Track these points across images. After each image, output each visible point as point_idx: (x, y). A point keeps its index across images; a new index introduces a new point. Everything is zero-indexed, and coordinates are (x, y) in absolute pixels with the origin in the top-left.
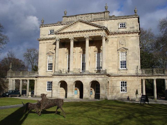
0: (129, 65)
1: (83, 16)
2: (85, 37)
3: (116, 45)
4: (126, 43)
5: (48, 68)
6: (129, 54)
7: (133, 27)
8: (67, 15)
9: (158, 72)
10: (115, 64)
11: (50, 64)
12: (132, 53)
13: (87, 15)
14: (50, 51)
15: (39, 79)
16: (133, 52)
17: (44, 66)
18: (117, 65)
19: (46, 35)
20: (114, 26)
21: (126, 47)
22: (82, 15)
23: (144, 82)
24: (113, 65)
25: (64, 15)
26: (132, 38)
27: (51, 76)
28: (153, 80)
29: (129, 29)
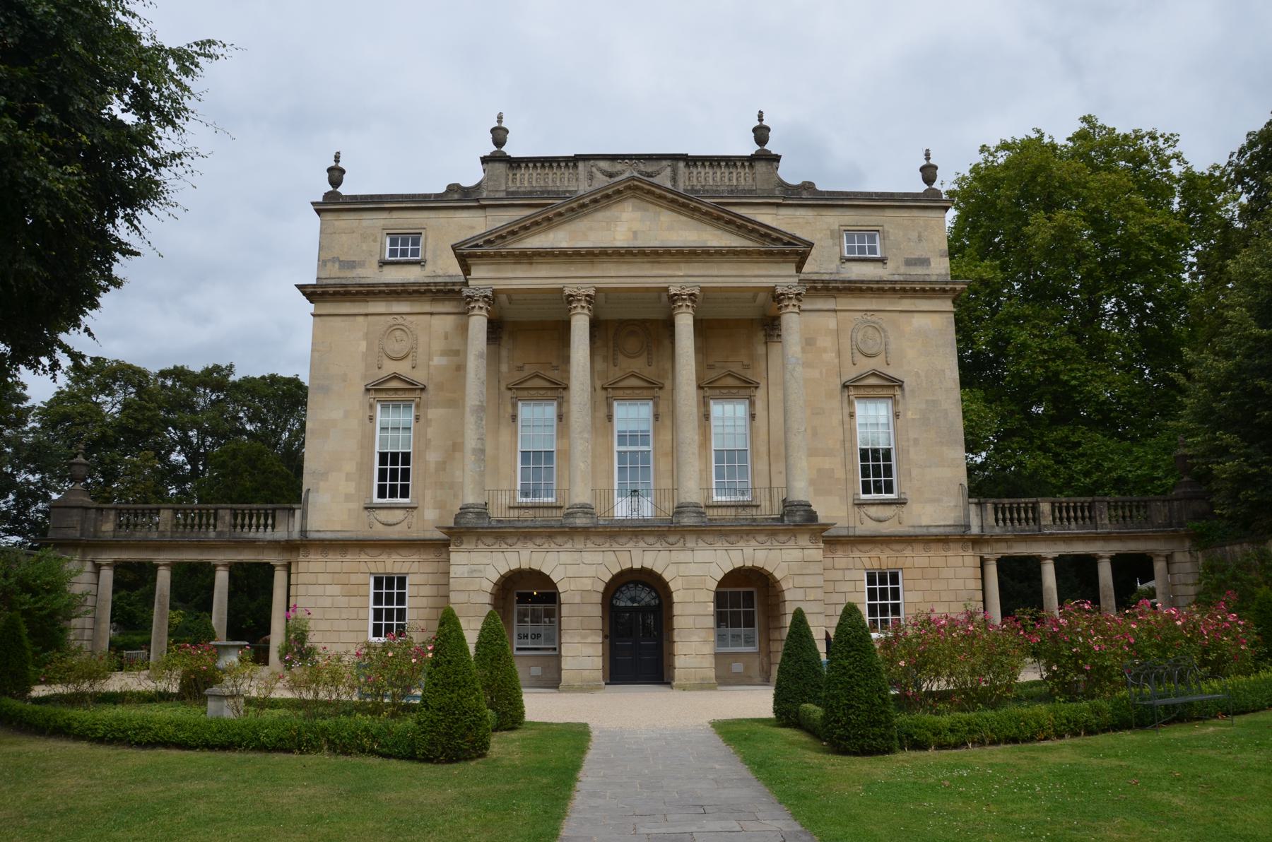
0: (915, 472)
1: (618, 166)
2: (673, 291)
3: (834, 354)
4: (892, 347)
5: (376, 483)
6: (912, 408)
7: (924, 262)
10: (827, 466)
11: (395, 455)
14: (390, 367)
15: (311, 567)
16: (927, 401)
17: (350, 467)
19: (362, 264)
21: (891, 372)
23: (992, 570)
24: (819, 470)
26: (919, 321)
27: (438, 535)
28: (1036, 562)
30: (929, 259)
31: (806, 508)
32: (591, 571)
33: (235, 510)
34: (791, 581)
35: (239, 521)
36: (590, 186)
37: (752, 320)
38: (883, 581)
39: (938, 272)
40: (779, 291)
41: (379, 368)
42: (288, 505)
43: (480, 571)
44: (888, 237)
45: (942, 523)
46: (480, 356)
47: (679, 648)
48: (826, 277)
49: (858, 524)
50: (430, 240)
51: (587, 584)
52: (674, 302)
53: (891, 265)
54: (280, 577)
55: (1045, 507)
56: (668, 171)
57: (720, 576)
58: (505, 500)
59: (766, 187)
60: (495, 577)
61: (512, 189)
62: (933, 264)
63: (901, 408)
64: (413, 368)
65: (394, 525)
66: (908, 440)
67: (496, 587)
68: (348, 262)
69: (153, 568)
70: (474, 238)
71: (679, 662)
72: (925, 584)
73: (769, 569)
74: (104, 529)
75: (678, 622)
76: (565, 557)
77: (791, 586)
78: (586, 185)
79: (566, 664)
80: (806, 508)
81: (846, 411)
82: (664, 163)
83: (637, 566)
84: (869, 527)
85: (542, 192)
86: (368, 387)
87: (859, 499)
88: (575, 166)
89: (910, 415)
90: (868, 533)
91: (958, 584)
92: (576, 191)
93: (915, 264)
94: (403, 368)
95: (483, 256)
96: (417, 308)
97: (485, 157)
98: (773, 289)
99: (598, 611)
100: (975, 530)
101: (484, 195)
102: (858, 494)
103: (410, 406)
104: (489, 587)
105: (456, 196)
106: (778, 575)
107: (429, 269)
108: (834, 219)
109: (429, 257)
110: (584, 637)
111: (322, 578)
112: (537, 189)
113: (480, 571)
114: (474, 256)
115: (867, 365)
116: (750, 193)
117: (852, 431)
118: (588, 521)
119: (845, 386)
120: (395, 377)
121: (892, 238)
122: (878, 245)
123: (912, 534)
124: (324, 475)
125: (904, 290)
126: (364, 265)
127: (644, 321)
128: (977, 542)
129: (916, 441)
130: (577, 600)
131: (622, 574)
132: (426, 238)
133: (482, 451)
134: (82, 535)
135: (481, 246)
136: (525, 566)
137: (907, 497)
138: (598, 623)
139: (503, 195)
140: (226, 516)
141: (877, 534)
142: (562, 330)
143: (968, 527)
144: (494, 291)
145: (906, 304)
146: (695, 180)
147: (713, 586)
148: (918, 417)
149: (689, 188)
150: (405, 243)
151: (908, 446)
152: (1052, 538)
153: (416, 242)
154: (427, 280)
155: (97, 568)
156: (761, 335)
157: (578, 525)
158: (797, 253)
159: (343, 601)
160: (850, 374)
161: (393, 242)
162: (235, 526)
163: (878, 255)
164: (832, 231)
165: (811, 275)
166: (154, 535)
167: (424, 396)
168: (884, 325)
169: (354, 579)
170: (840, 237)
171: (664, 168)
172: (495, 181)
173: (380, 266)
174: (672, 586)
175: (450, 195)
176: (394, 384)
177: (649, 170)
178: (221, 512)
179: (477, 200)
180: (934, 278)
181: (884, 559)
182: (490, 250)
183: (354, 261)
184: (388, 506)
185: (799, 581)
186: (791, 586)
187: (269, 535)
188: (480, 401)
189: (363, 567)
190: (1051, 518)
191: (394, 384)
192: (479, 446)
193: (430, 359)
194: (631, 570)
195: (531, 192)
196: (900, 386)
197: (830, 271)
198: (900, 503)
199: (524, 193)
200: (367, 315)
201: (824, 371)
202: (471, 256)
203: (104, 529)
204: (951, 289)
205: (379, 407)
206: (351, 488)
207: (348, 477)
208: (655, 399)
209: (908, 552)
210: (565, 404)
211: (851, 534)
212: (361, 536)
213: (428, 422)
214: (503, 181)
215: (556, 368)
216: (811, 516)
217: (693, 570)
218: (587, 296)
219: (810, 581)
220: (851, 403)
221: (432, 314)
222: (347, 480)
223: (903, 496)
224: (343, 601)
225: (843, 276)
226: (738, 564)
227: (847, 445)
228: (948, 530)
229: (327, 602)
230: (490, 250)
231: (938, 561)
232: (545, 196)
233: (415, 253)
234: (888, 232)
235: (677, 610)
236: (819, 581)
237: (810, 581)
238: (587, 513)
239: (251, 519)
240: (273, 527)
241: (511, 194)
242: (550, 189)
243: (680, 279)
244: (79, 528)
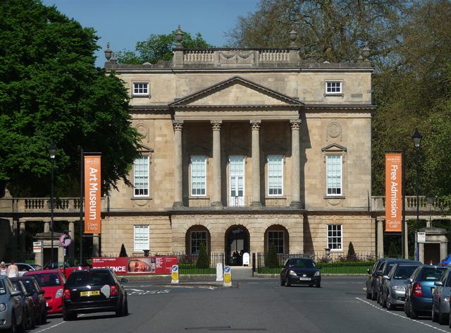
0: (349, 186)
1: (231, 53)
7: (360, 95)
10: (314, 183)
12: (355, 158)
18: (319, 186)
20: (314, 88)
21: (342, 144)
26: (356, 122)
29: (350, 99)
30: (362, 95)
38: (334, 229)
49: (325, 206)
53: (345, 98)
56: (252, 56)
62: (364, 97)
69: (43, 223)
72: (351, 230)
82: (251, 51)
85: (199, 65)
89: (349, 162)
92: (213, 64)
96: (149, 116)
100: (373, 209)
103: (147, 158)
122: (341, 87)
129: (350, 173)
138: (224, 245)
139: (182, 66)
145: (350, 115)
150: (141, 86)
154: (152, 105)
163: (341, 92)
167: (153, 154)
170: (325, 85)
177: (244, 55)
178: (70, 201)
180: (364, 103)
181: (334, 220)
185: (294, 230)
193: (155, 138)
196: (346, 151)
198: (343, 198)
209: (345, 217)
213: (155, 165)
217: (257, 225)
231: (357, 222)
241: (187, 66)
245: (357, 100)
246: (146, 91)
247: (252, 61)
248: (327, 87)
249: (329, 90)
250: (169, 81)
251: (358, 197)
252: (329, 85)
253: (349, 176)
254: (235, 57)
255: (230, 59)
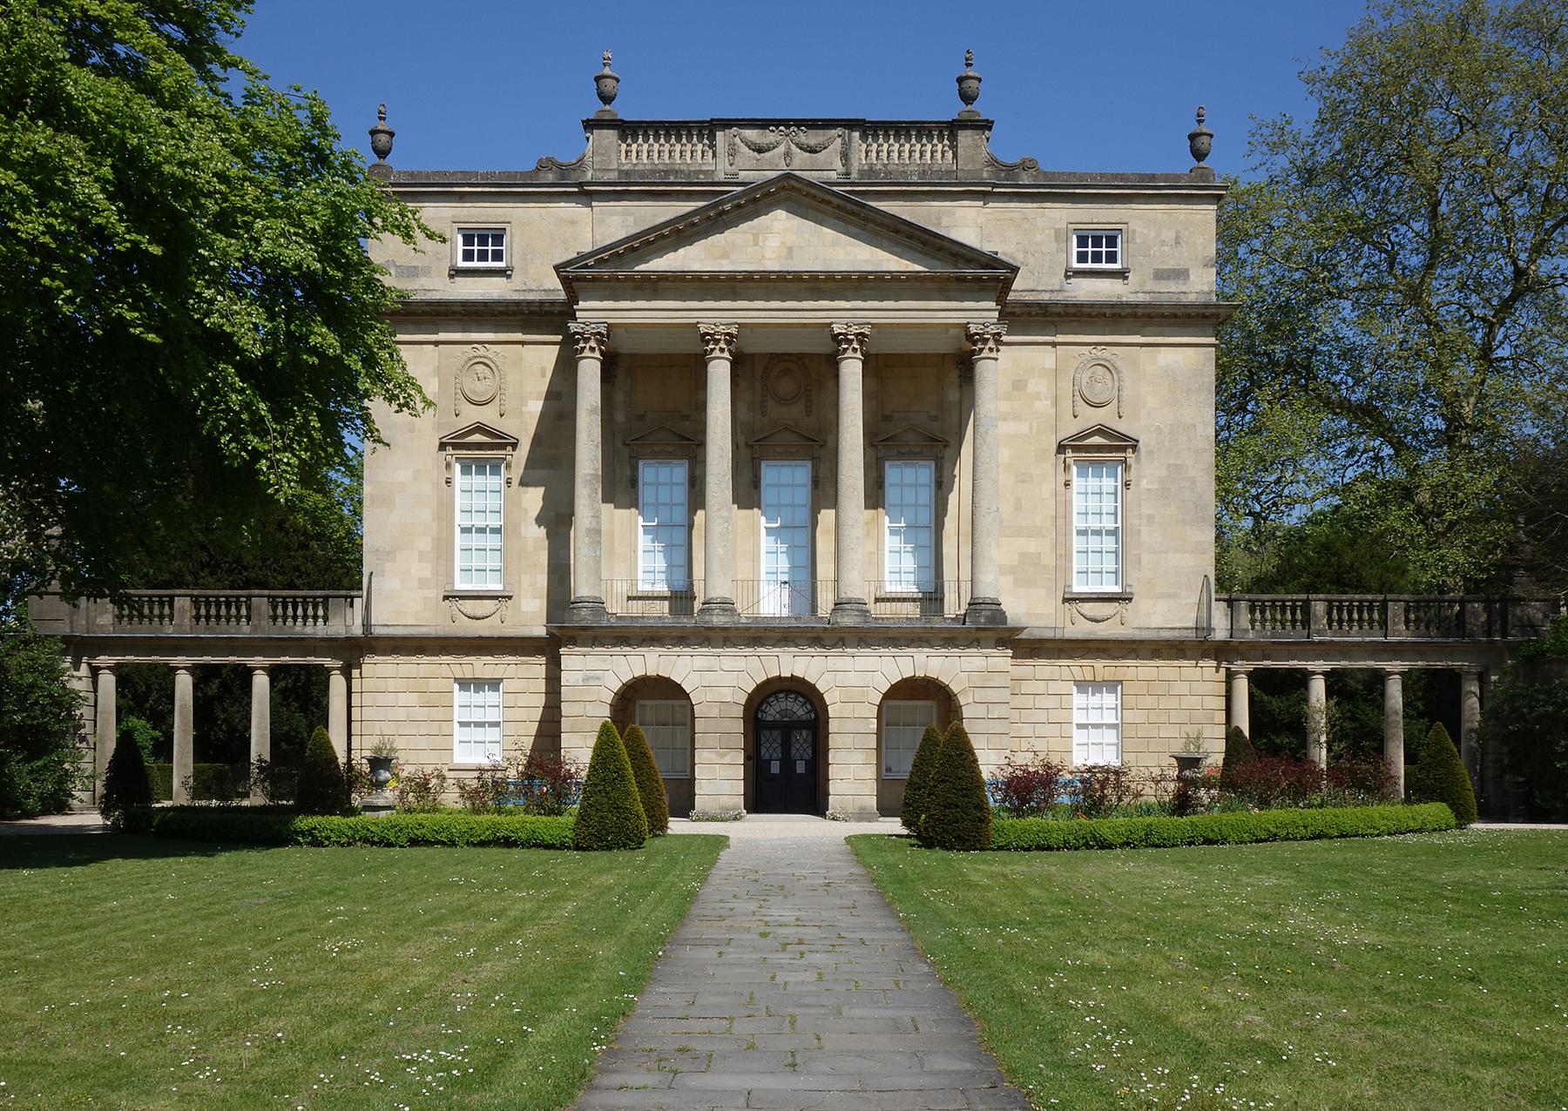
0: (1145, 558)
1: (769, 137)
4: (1125, 394)
7: (1180, 274)
8: (623, 110)
9: (1340, 621)
10: (1032, 549)
12: (1164, 473)
13: (812, 138)
14: (472, 415)
15: (376, 669)
16: (1169, 466)
17: (425, 543)
18: (1049, 560)
19: (427, 271)
21: (1122, 427)
22: (763, 124)
23: (1242, 686)
24: (1022, 555)
25: (594, 109)
30: (1187, 271)
31: (994, 607)
32: (731, 679)
33: (274, 597)
34: (971, 694)
35: (280, 611)
36: (731, 165)
37: (944, 354)
39: (1198, 288)
40: (973, 330)
41: (457, 415)
42: (343, 592)
43: (598, 679)
44: (1134, 239)
45: (1178, 625)
46: (592, 411)
47: (833, 772)
48: (1045, 297)
50: (517, 239)
51: (727, 695)
52: (839, 343)
54: (337, 683)
55: (1319, 608)
57: (885, 688)
58: (622, 589)
59: (970, 167)
60: (617, 686)
61: (626, 167)
62: (1192, 277)
63: (1133, 475)
64: (501, 415)
65: (483, 618)
66: (1140, 517)
67: (617, 697)
68: (408, 268)
70: (582, 257)
71: (833, 787)
72: (1150, 702)
73: (945, 680)
74: (100, 621)
75: (834, 741)
76: (700, 662)
77: (970, 700)
78: (727, 164)
79: (700, 789)
80: (994, 607)
81: (1062, 479)
83: (786, 674)
84: (1081, 629)
86: (444, 440)
87: (1072, 593)
88: (712, 137)
89: (1144, 484)
90: (1080, 636)
91: (1194, 702)
93: (1169, 278)
94: (487, 416)
95: (594, 279)
97: (588, 120)
98: (966, 326)
99: (739, 727)
100: (1220, 633)
101: (589, 176)
102: (1070, 586)
104: (609, 697)
105: (551, 177)
106: (955, 688)
107: (517, 280)
108: (1061, 215)
109: (516, 263)
110: (723, 756)
111: (392, 685)
112: (660, 167)
113: (598, 679)
114: (584, 279)
115: (1093, 417)
116: (950, 177)
117: (1068, 504)
118: (728, 619)
119: (1061, 448)
120: (480, 428)
121: (1138, 240)
123: (1136, 638)
124: (390, 554)
125: (1149, 316)
126: (430, 272)
127: (801, 357)
128: (1221, 652)
129: (1150, 518)
130: (715, 713)
131: (768, 682)
132: (512, 237)
133: (598, 532)
134: (72, 631)
135: (591, 267)
136: (651, 673)
137: (1133, 590)
139: (613, 176)
140: (261, 604)
141: (1092, 637)
142: (696, 366)
143: (1210, 629)
144: (610, 327)
146: (874, 155)
147: (877, 699)
148: (1156, 487)
149: (866, 168)
151: (1140, 525)
152: (1323, 651)
153: (498, 239)
155: (95, 672)
156: (954, 376)
157: (715, 624)
158: (997, 279)
159: (421, 713)
160: (1071, 428)
161: (468, 240)
162: (275, 618)
164: (1057, 231)
165: (1024, 294)
166: (169, 631)
168: (1118, 364)
169: (434, 685)
170: (1068, 240)
171: (832, 140)
172: (602, 155)
173: (451, 276)
174: (828, 699)
175: (541, 175)
176: (477, 438)
179: (581, 185)
180: (1192, 298)
182: (605, 272)
183: (416, 267)
184: (476, 594)
185: (980, 695)
186: (970, 700)
187: (319, 630)
188: (596, 469)
189: (445, 671)
190: (1325, 621)
191: (477, 438)
192: (594, 525)
194: (780, 678)
195: (653, 172)
196: (1134, 448)
197: (1050, 288)
199: (642, 173)
200: (436, 343)
201: (1035, 424)
202: (578, 279)
203: (100, 621)
204: (1212, 315)
205: (458, 467)
206: (425, 571)
207: (422, 557)
208: (816, 461)
210: (699, 466)
211: (1058, 636)
212: (441, 632)
214: (614, 156)
215: (687, 418)
216: (998, 615)
217: (853, 679)
218: (727, 334)
219: (992, 695)
220: (1067, 468)
221: (523, 343)
222: (420, 561)
223: (1128, 590)
224: (421, 713)
225: (1067, 294)
226: (908, 674)
227: (1060, 522)
228: (1185, 633)
229: (401, 714)
230: (605, 272)
232: (672, 179)
233: (498, 256)
234: (1134, 231)
235: (833, 726)
236: (1005, 695)
237: (992, 695)
238: (726, 610)
239: (295, 609)
240: (326, 618)
241: (627, 177)
242: (677, 167)
243: (844, 315)
244: (68, 622)
245: (1170, 291)
246: (498, 256)
247: (838, 165)
248: (1075, 249)
249: (1082, 257)
250: (573, 222)
251: (1174, 596)
252: (1082, 242)
253: (1144, 530)
254: (781, 149)
255: (767, 155)
